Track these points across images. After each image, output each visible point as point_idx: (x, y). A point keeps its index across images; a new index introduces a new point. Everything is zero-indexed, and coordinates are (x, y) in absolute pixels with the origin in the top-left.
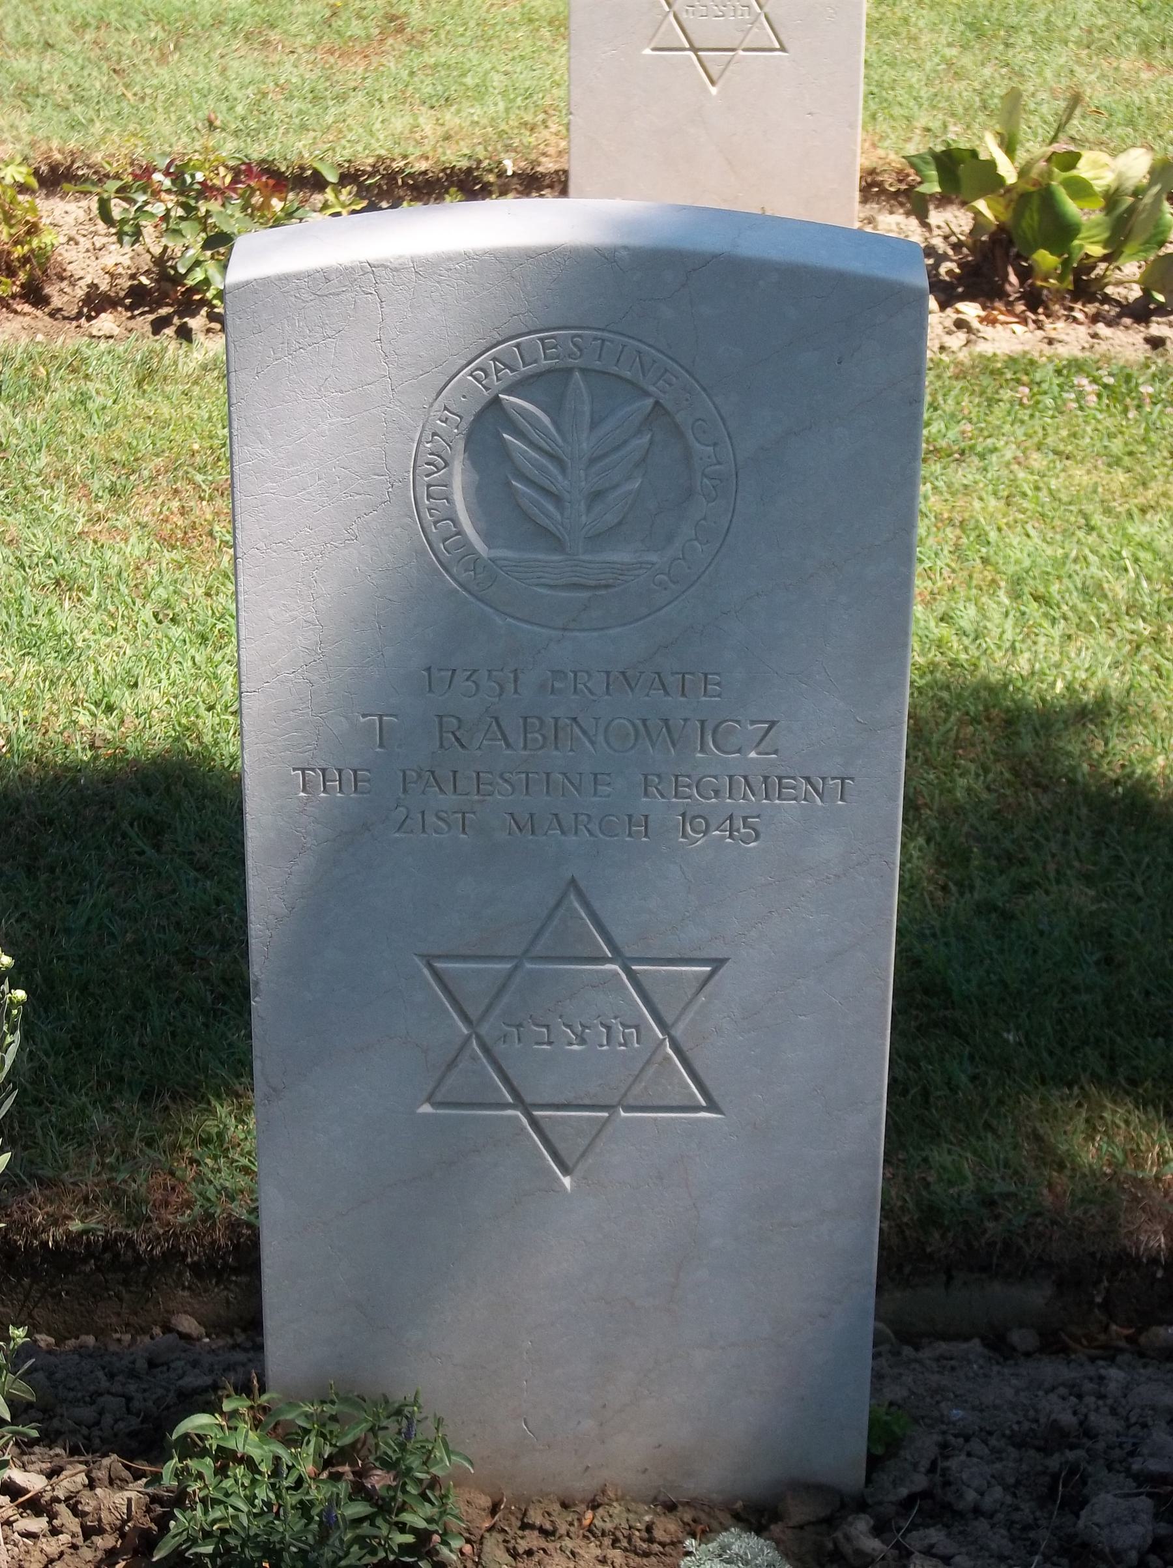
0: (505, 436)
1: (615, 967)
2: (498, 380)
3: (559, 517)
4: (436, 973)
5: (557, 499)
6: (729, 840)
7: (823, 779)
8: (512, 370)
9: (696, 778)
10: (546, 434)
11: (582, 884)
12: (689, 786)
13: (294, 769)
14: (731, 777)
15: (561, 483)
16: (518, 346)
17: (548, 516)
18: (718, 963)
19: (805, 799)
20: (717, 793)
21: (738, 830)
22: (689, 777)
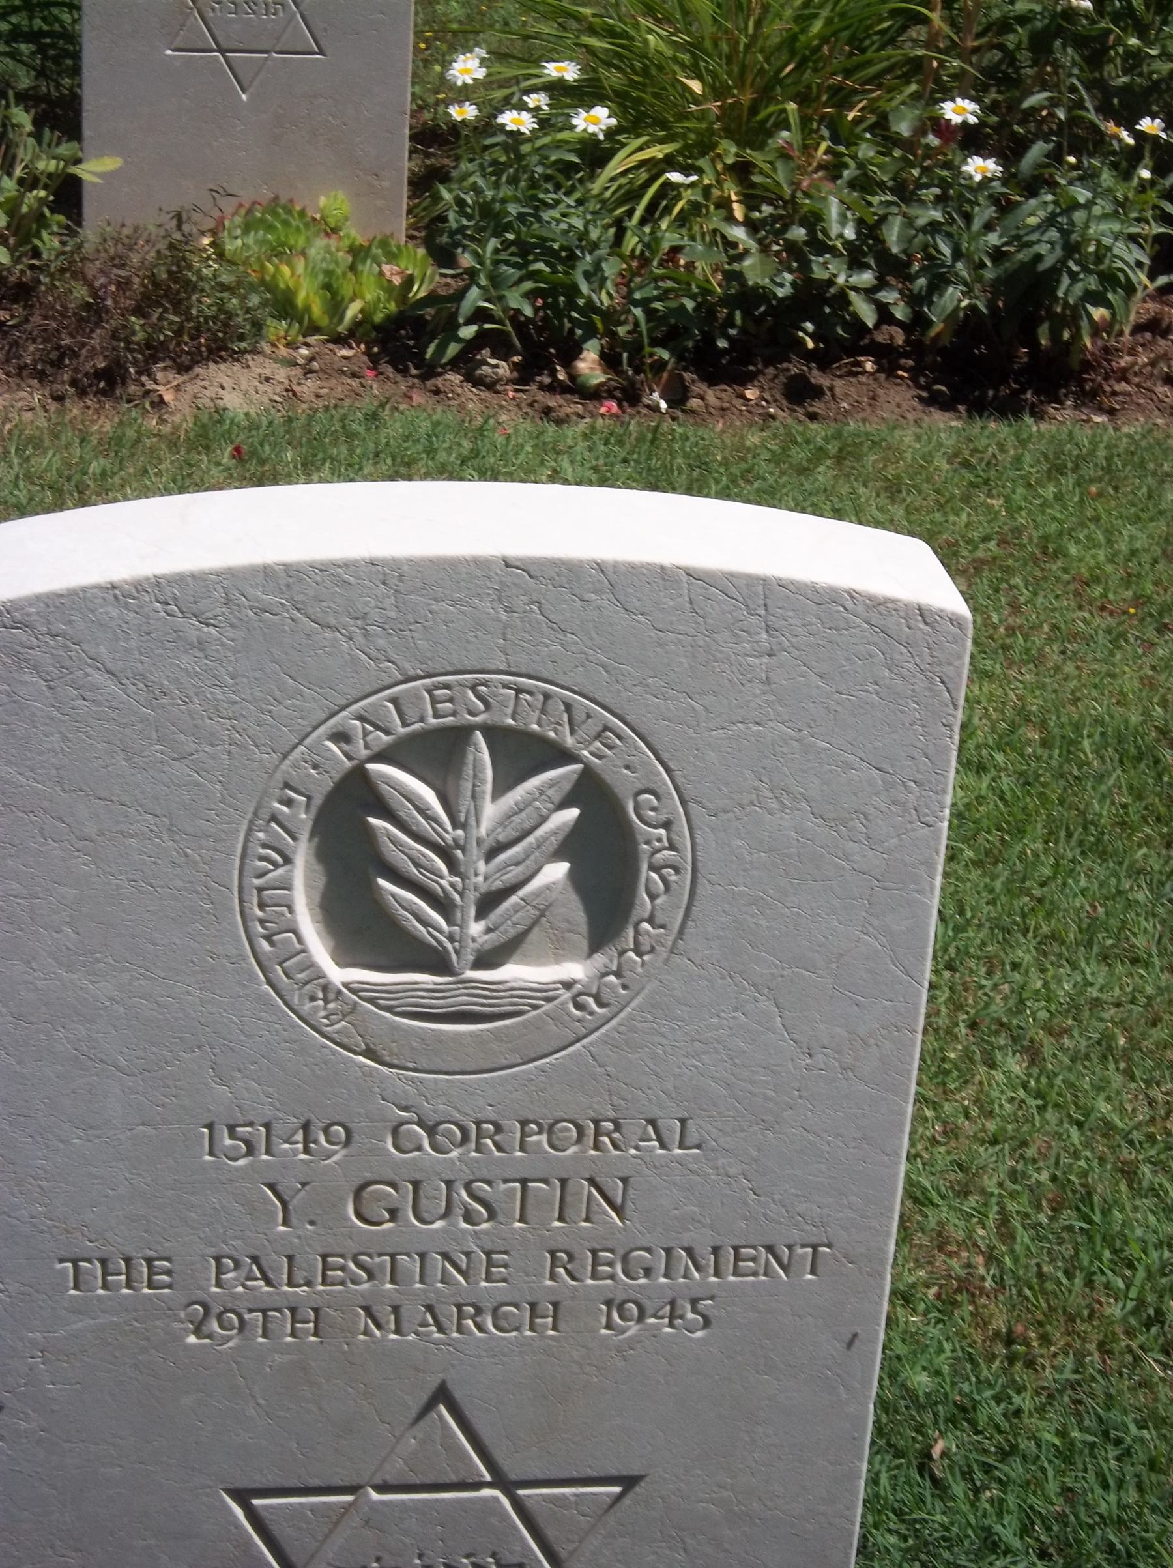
0: (372, 820)
1: (497, 1493)
2: (367, 747)
3: (442, 922)
4: (253, 1515)
6: (668, 1330)
7: (790, 1247)
8: (387, 732)
9: (622, 1252)
10: (431, 818)
11: (458, 1394)
12: (610, 1264)
13: (61, 1261)
14: (668, 1251)
15: (446, 881)
16: (394, 700)
17: (426, 923)
18: (629, 1482)
19: (765, 1274)
20: (648, 1272)
21: (682, 1317)
22: (611, 1251)
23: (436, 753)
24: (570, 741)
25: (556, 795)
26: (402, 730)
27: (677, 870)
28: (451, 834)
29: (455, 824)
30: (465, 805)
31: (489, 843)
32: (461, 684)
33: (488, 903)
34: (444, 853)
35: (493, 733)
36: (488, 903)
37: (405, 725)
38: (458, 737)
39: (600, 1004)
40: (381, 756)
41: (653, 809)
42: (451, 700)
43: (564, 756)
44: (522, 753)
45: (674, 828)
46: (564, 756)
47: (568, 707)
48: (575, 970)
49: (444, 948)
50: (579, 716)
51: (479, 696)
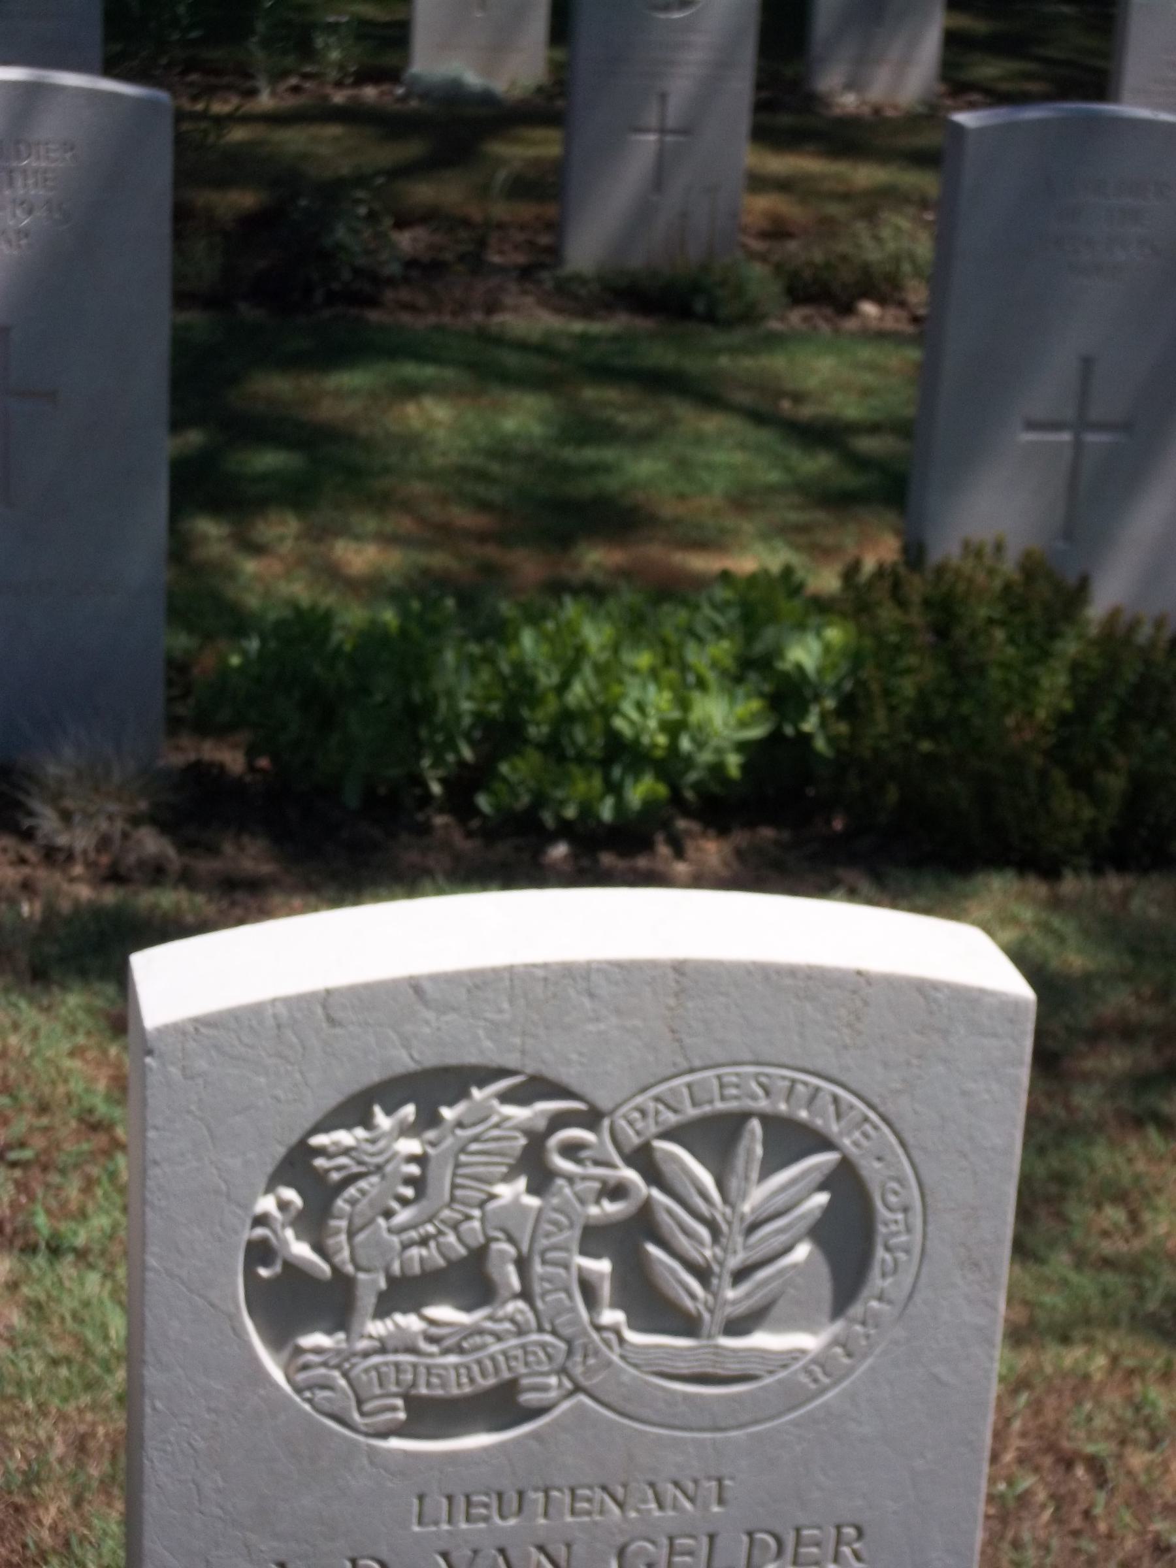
2: (657, 1123)
5: (702, 1274)
8: (675, 1111)
23: (715, 1136)
24: (835, 1128)
25: (817, 1177)
26: (692, 1112)
27: (907, 1251)
28: (720, 1210)
29: (726, 1200)
30: (734, 1184)
31: (749, 1219)
32: (747, 1075)
33: (740, 1276)
34: (711, 1225)
35: (767, 1120)
36: (740, 1276)
37: (695, 1104)
38: (740, 1119)
39: (826, 1374)
40: (668, 1135)
41: (896, 1193)
42: (737, 1086)
43: (824, 1143)
44: (790, 1139)
45: (910, 1214)
46: (824, 1143)
47: (836, 1099)
48: (807, 1341)
49: (700, 1316)
50: (844, 1107)
51: (761, 1085)
